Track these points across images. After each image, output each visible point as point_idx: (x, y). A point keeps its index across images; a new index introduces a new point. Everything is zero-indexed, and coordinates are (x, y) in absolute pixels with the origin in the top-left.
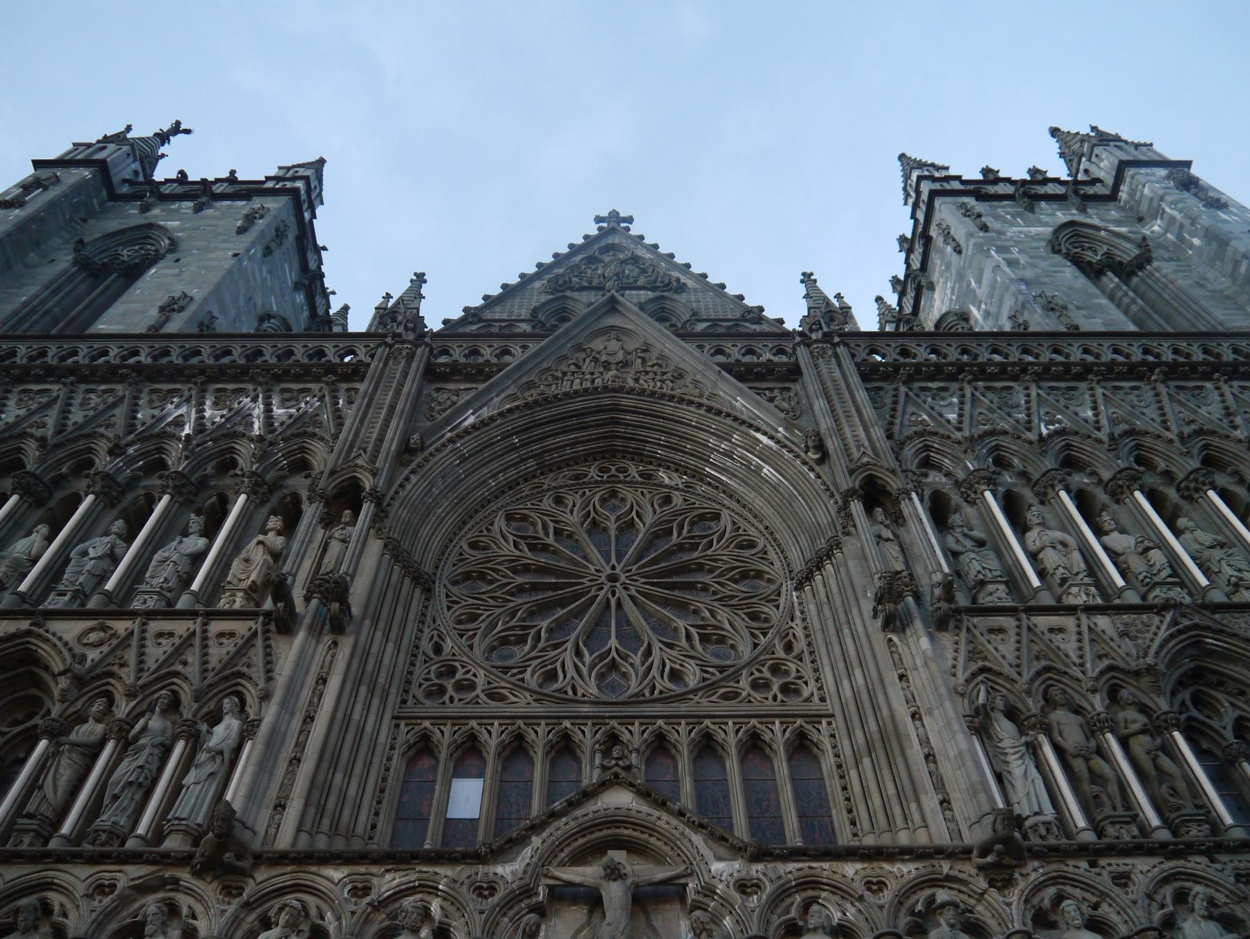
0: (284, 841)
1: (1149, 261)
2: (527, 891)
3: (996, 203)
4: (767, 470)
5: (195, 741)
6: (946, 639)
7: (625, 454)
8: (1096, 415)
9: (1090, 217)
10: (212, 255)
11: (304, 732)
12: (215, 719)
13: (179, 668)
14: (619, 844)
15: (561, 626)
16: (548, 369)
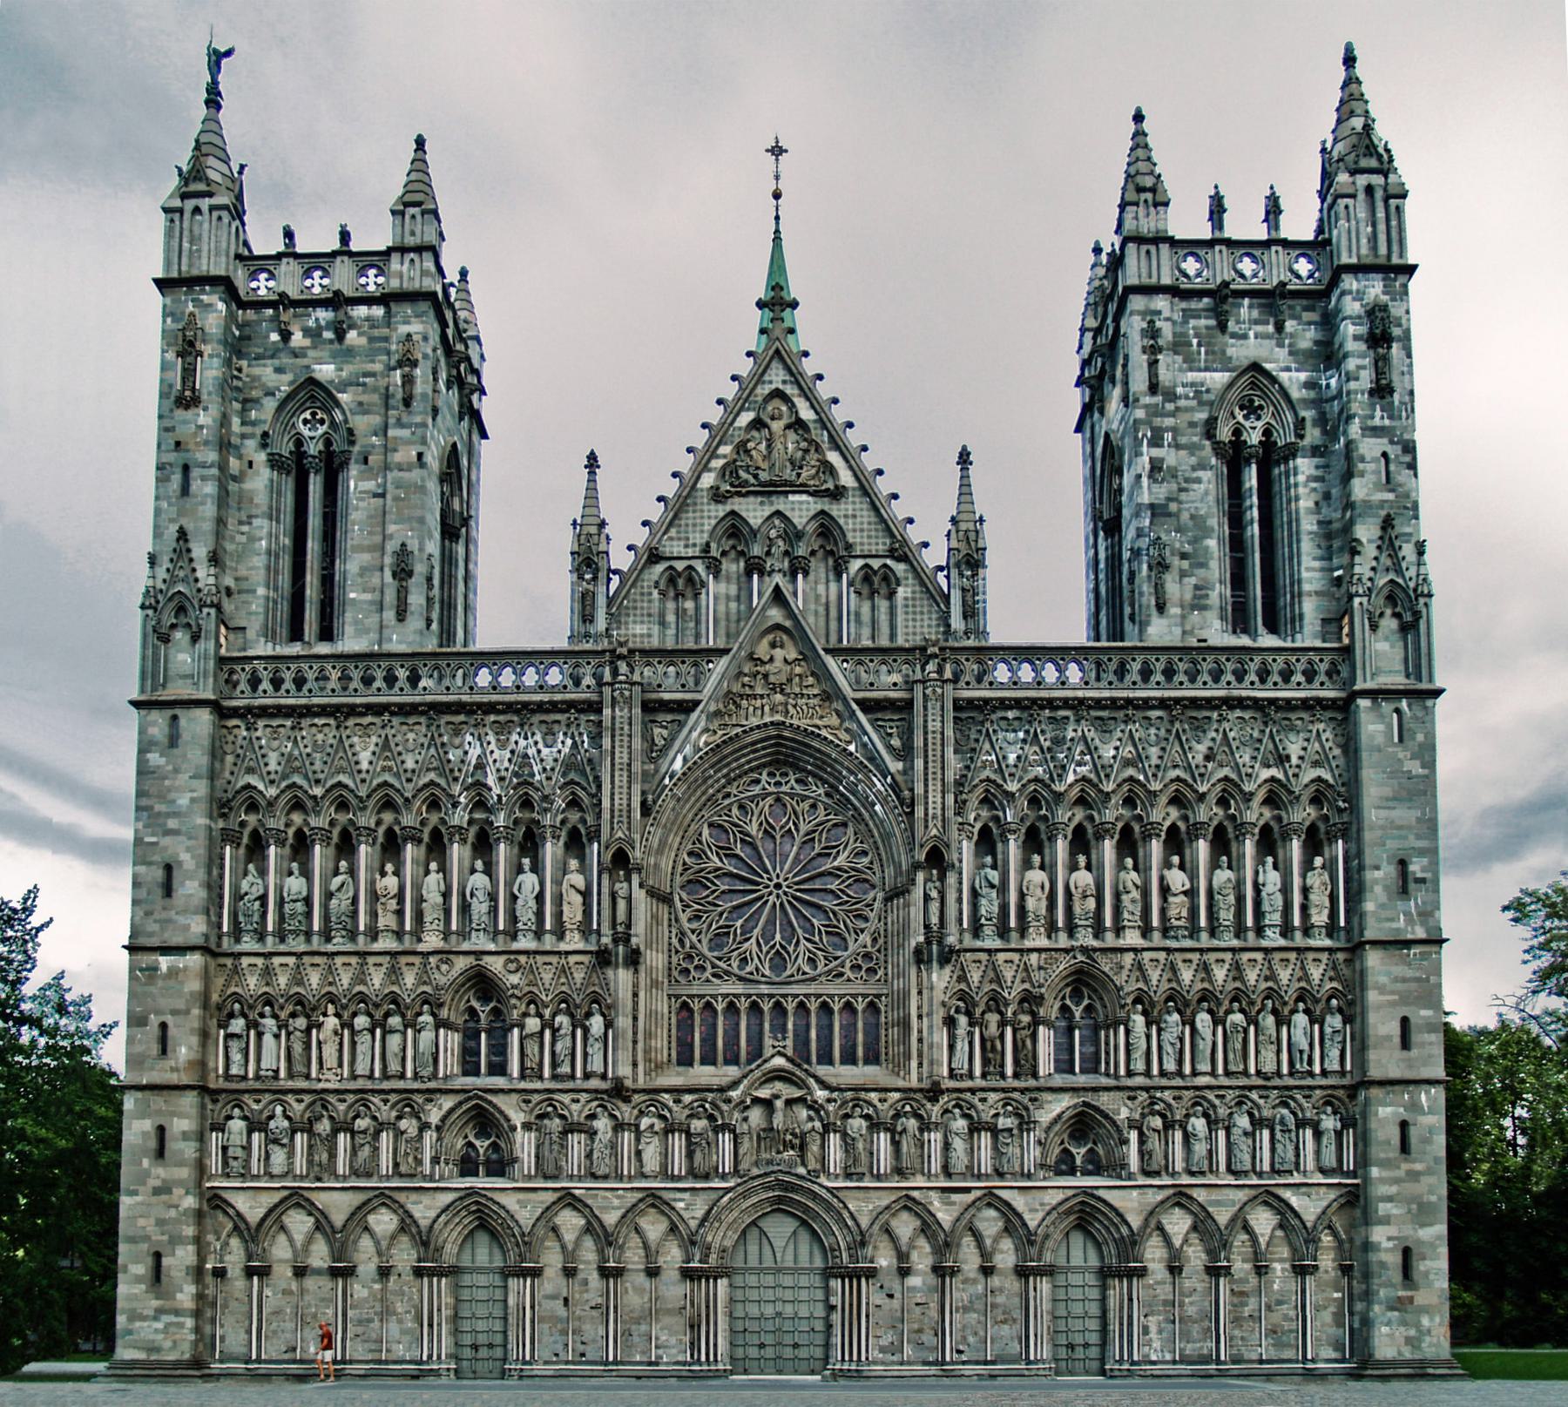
0: (641, 1082)
1: (1294, 457)
2: (743, 1102)
3: (1194, 304)
4: (878, 808)
5: (586, 1031)
6: (948, 970)
7: (785, 763)
8: (1114, 757)
9: (1280, 345)
10: (398, 457)
11: (635, 1026)
12: (589, 1015)
13: (564, 988)
14: (780, 1078)
15: (747, 931)
16: (729, 692)
